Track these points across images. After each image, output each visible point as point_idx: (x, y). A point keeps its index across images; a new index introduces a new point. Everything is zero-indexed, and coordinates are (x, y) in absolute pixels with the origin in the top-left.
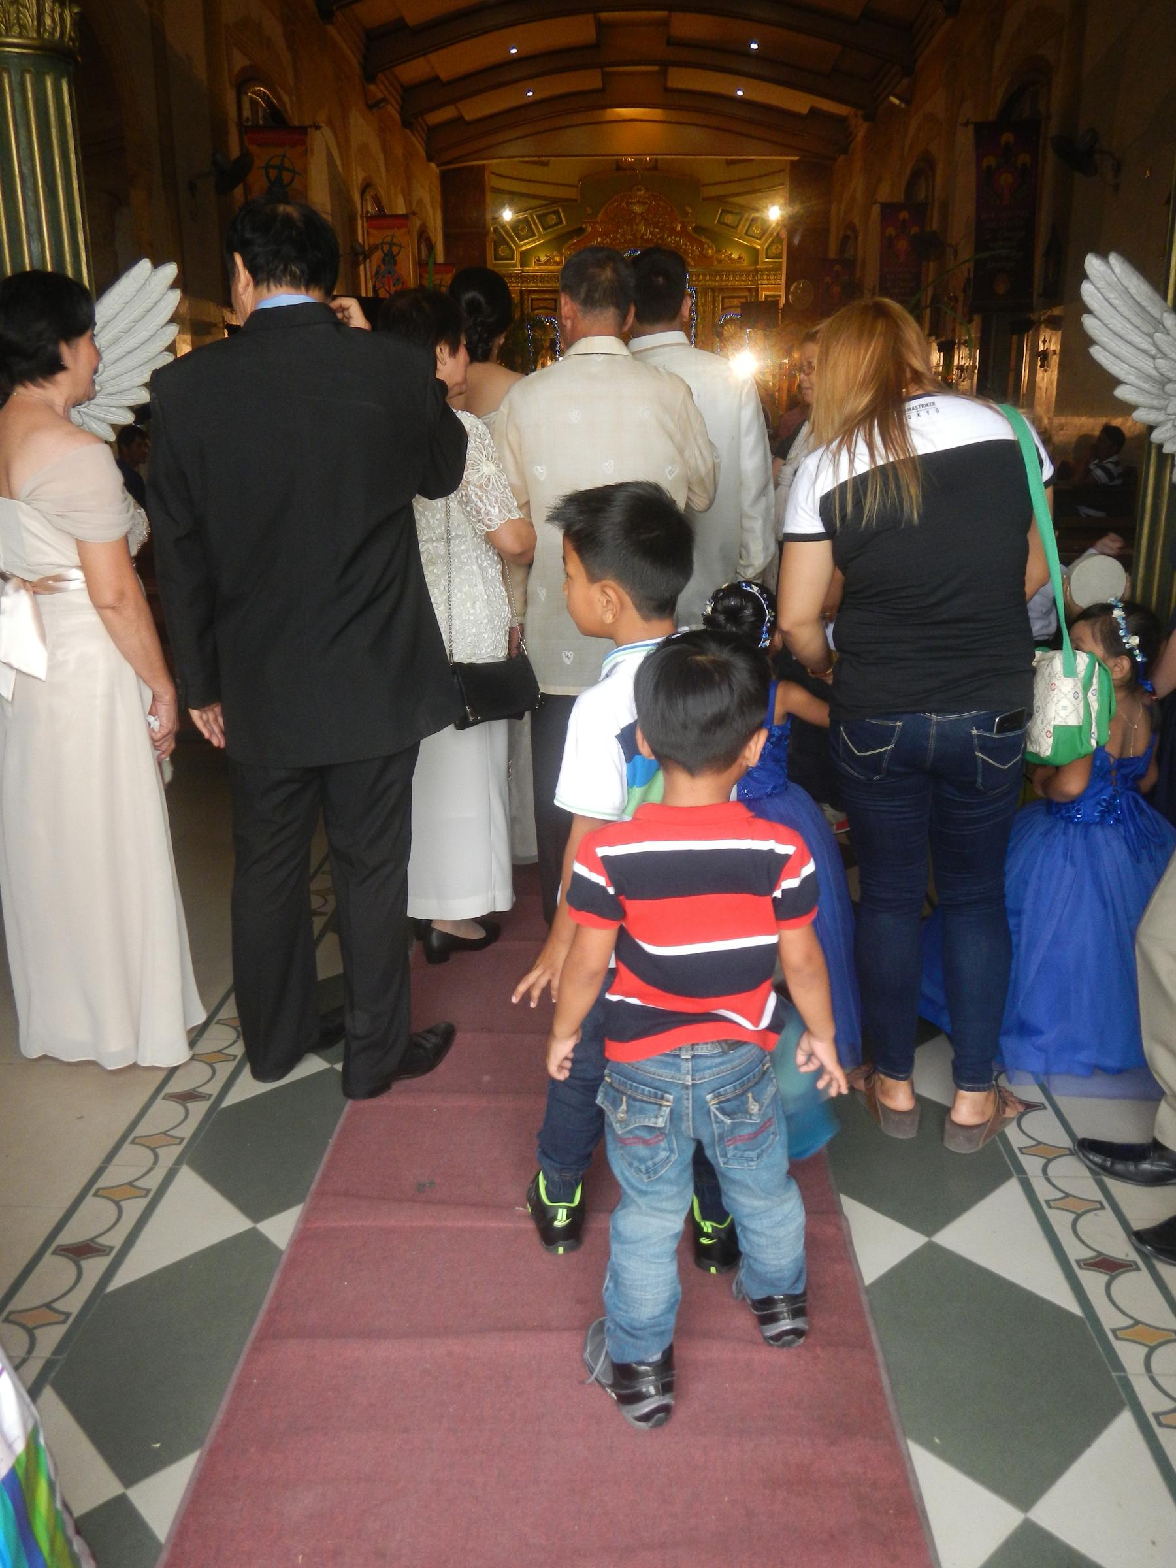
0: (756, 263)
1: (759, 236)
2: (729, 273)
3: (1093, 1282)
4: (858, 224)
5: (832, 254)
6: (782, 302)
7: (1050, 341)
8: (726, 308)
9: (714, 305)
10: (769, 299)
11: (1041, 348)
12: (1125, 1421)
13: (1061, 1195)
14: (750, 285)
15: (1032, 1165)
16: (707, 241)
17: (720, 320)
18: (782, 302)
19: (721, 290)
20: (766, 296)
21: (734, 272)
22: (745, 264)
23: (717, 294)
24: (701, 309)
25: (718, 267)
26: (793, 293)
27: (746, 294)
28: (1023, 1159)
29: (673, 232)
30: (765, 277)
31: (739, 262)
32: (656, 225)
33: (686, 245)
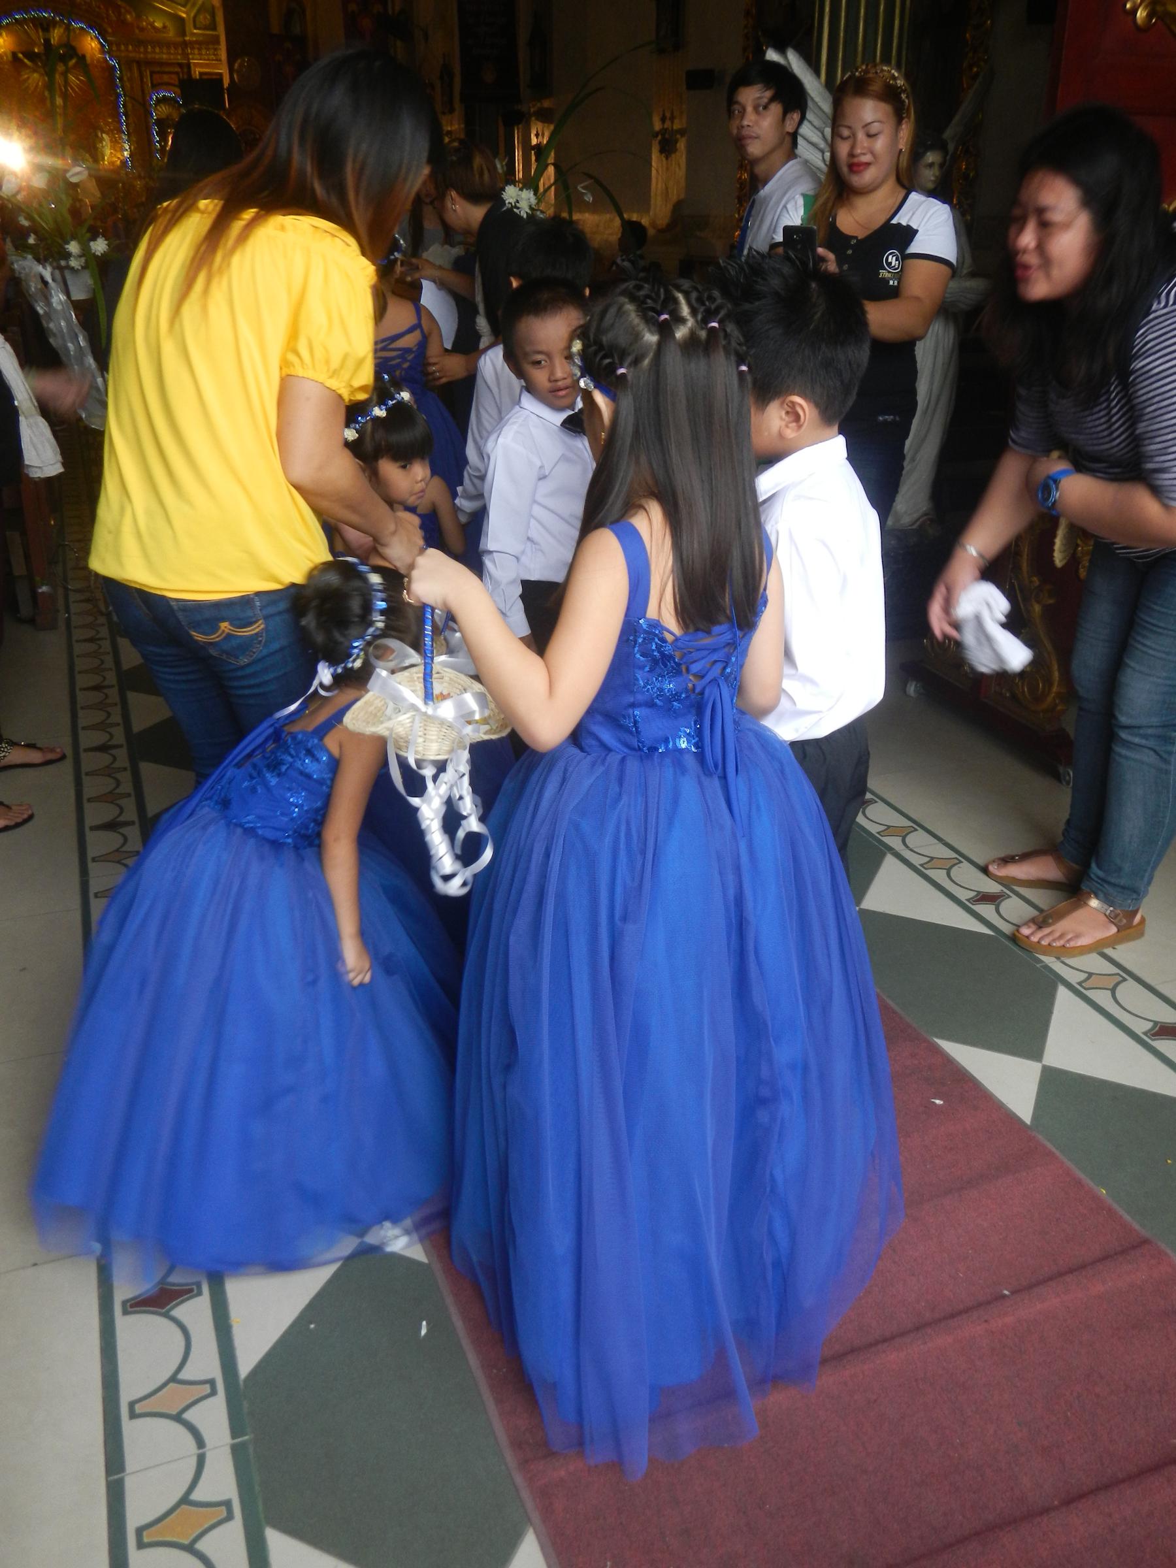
0: (184, 34)
3: (986, 910)
5: (276, 29)
6: (226, 82)
7: (543, 135)
9: (142, 80)
10: (205, 77)
11: (534, 141)
12: (1062, 992)
13: (928, 859)
14: (180, 59)
15: (894, 842)
17: (151, 99)
18: (226, 82)
19: (149, 63)
20: (201, 74)
21: (159, 43)
22: (171, 34)
23: (143, 69)
24: (128, 84)
27: (177, 69)
28: (886, 840)
30: (196, 51)
33: (99, 7)
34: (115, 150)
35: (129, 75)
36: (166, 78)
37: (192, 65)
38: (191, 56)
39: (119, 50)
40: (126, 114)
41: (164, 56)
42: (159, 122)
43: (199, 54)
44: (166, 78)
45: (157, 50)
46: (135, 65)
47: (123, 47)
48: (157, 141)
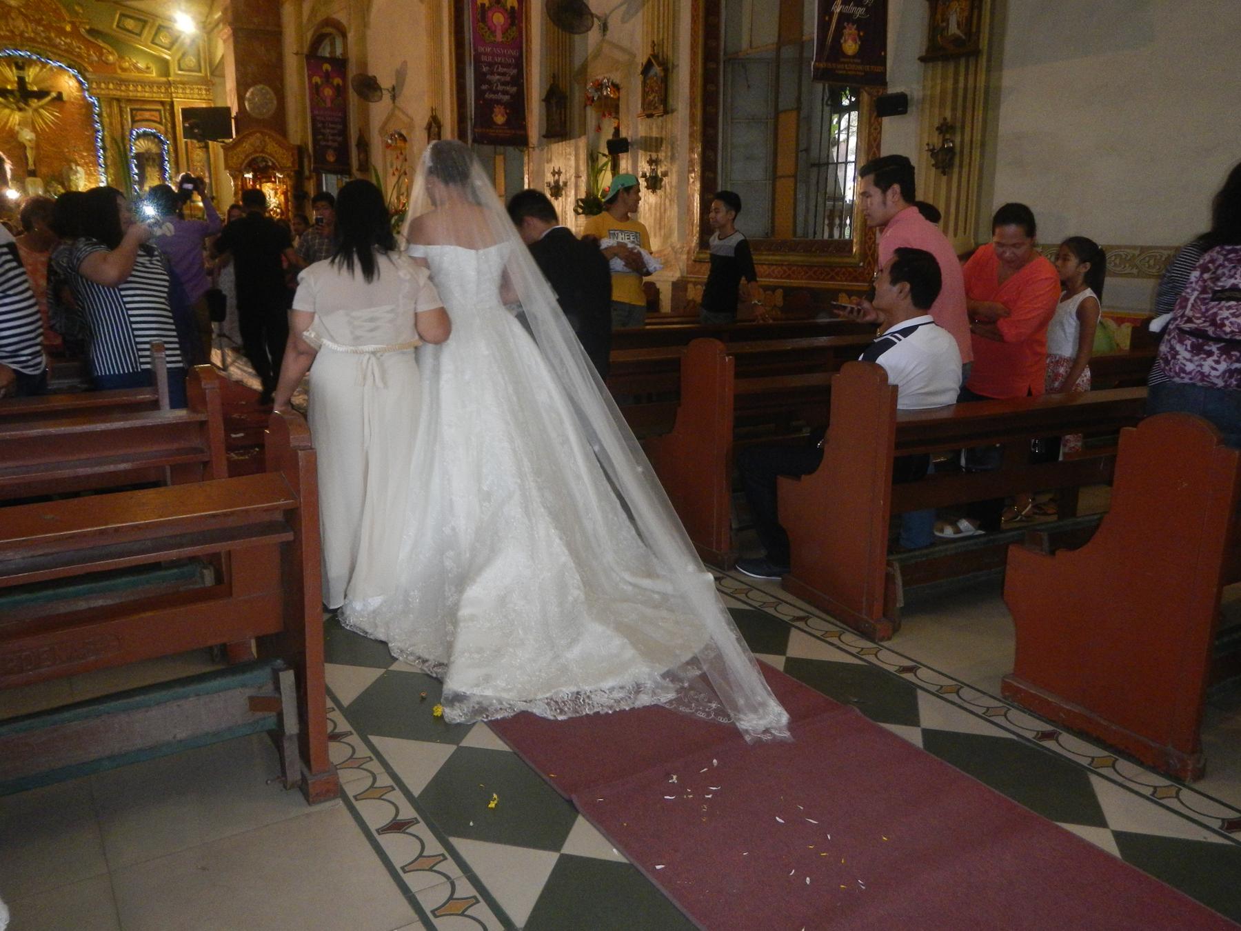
0: (167, 74)
1: (168, 46)
2: (138, 82)
4: (344, 21)
8: (138, 121)
9: (121, 116)
14: (163, 98)
16: (106, 46)
17: (131, 134)
19: (129, 101)
22: (154, 75)
24: (106, 120)
25: (124, 75)
26: (249, 100)
29: (62, 32)
30: (180, 91)
31: (147, 73)
32: (39, 22)
33: (80, 48)
34: (90, 182)
35: (108, 110)
36: (147, 115)
37: (175, 103)
38: (174, 95)
39: (99, 87)
40: (104, 149)
41: (147, 95)
42: (138, 156)
43: (182, 93)
44: (147, 115)
45: (139, 88)
46: (115, 103)
47: (103, 85)
48: (136, 174)
